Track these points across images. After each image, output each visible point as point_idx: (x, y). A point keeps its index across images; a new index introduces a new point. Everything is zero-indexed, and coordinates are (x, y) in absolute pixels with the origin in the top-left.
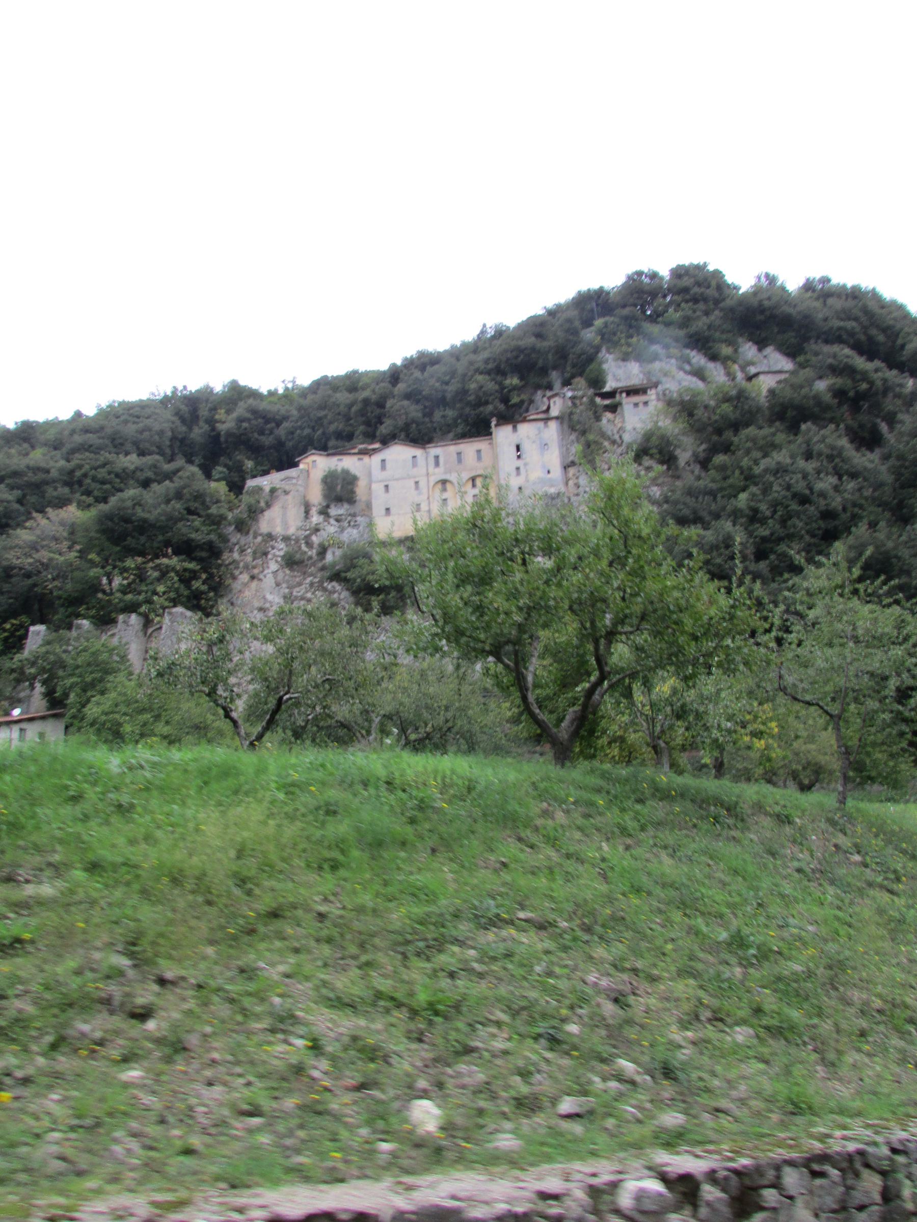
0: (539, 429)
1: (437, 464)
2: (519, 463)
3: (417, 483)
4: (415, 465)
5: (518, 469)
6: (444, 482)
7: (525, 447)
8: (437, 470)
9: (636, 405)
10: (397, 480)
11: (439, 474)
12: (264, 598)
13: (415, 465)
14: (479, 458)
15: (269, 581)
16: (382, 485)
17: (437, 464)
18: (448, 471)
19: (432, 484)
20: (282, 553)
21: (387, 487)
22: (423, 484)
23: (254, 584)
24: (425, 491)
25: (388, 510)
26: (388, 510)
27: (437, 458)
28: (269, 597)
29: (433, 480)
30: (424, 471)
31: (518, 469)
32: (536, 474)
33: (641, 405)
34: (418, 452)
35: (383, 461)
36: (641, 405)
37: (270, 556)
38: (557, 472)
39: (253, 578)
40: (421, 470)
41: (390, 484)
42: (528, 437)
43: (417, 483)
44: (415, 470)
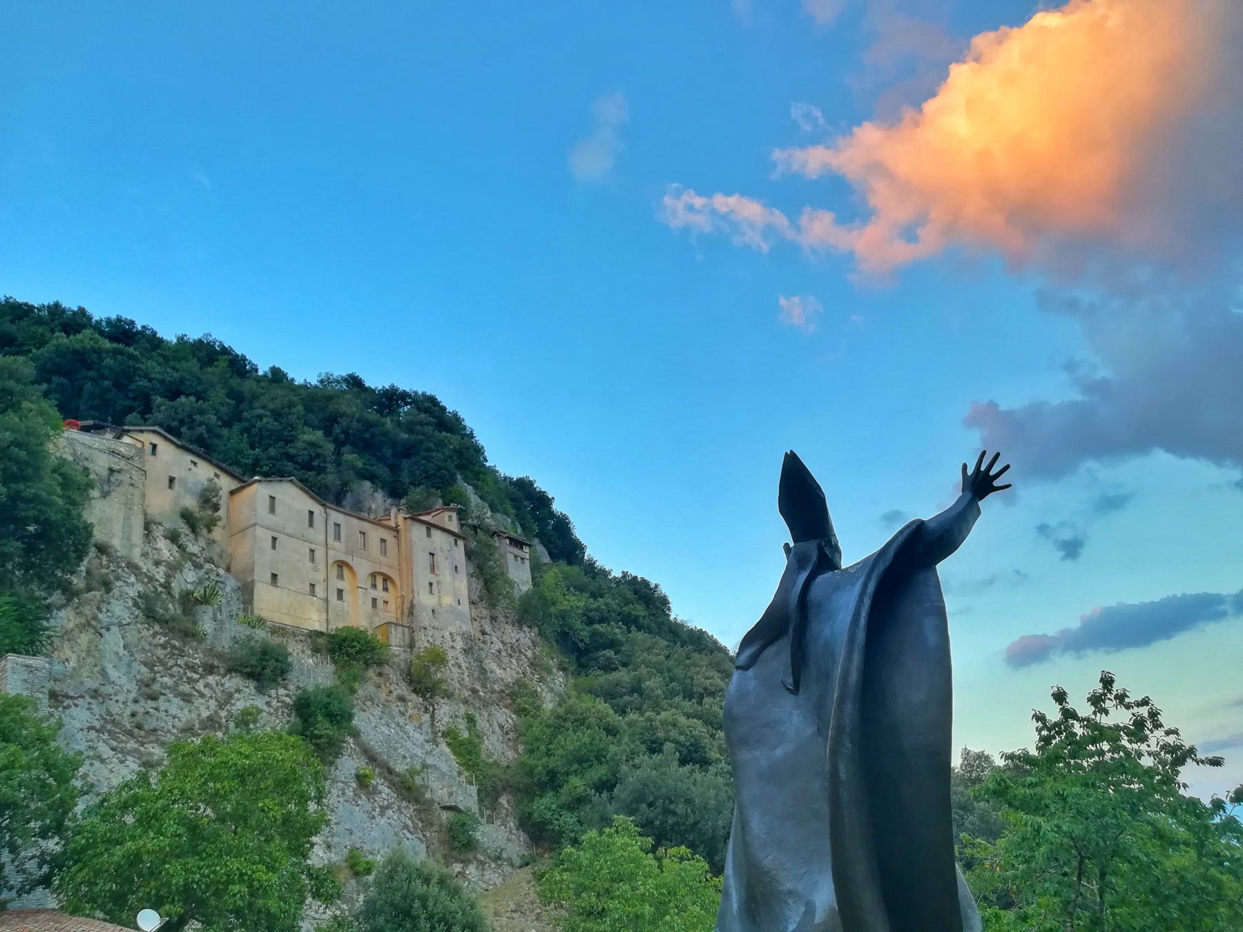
0: (450, 544)
1: (338, 537)
2: (433, 578)
3: (312, 551)
4: (311, 524)
5: (431, 584)
6: (341, 565)
7: (439, 558)
8: (337, 544)
9: (516, 556)
10: (290, 536)
11: (338, 550)
12: (103, 672)
13: (311, 524)
14: (384, 552)
15: (113, 641)
16: (270, 534)
17: (338, 537)
18: (349, 552)
19: (330, 562)
20: (132, 592)
21: (274, 539)
22: (320, 554)
23: (84, 639)
24: (322, 567)
25: (274, 576)
26: (274, 576)
27: (337, 525)
28: (113, 674)
29: (334, 555)
30: (322, 538)
31: (431, 584)
32: (448, 600)
33: (519, 558)
34: (317, 509)
35: (272, 498)
36: (519, 558)
37: (116, 592)
38: (465, 607)
39: (88, 625)
40: (317, 534)
41: (281, 537)
42: (441, 548)
43: (312, 551)
44: (311, 530)
